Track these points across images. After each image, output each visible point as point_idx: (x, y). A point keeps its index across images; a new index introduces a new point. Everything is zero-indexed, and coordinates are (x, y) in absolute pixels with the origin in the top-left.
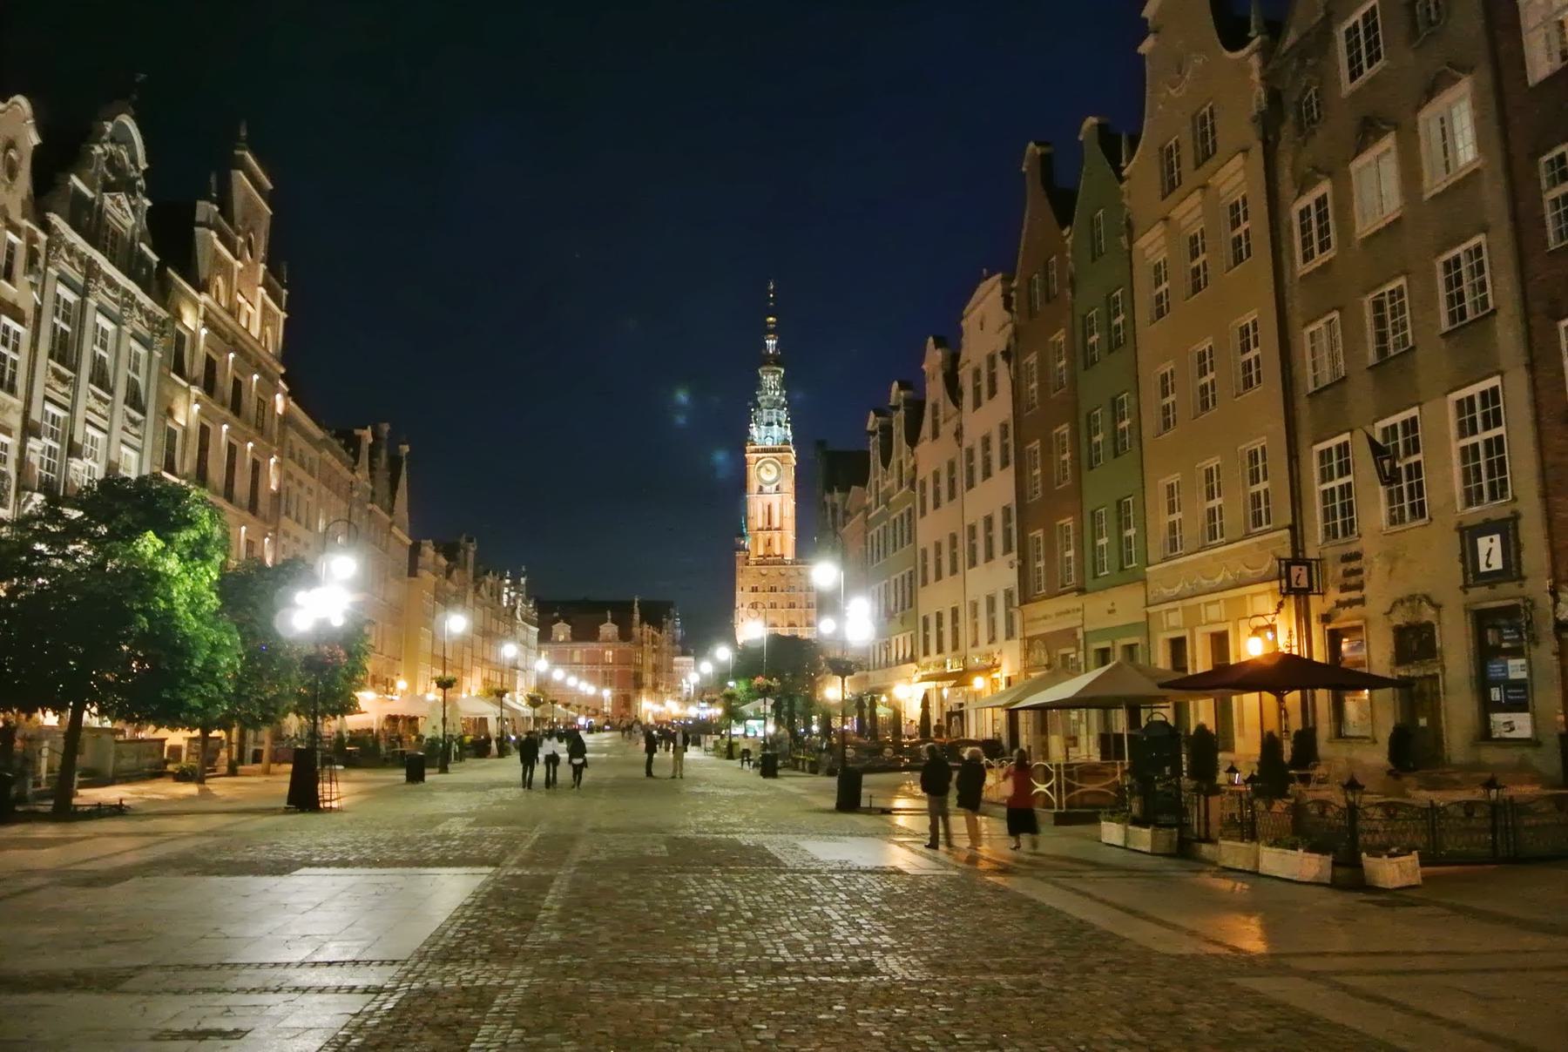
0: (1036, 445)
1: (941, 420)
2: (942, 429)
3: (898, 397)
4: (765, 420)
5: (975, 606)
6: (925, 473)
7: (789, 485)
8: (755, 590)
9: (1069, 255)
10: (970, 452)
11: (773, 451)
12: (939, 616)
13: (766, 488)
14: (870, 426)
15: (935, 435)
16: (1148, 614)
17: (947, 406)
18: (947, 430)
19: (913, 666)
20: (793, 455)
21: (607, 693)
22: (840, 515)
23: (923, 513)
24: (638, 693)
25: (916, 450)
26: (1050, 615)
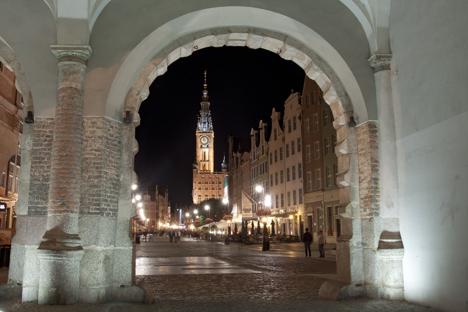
0: (309, 146)
1: (277, 135)
2: (278, 137)
3: (262, 125)
4: (203, 121)
5: (289, 193)
6: (271, 151)
7: (211, 145)
8: (200, 183)
10: (287, 146)
11: (206, 132)
13: (204, 146)
14: (251, 134)
15: (275, 139)
18: (279, 138)
20: (213, 134)
21: (148, 220)
22: (239, 161)
23: (271, 163)
24: (157, 220)
26: (313, 197)
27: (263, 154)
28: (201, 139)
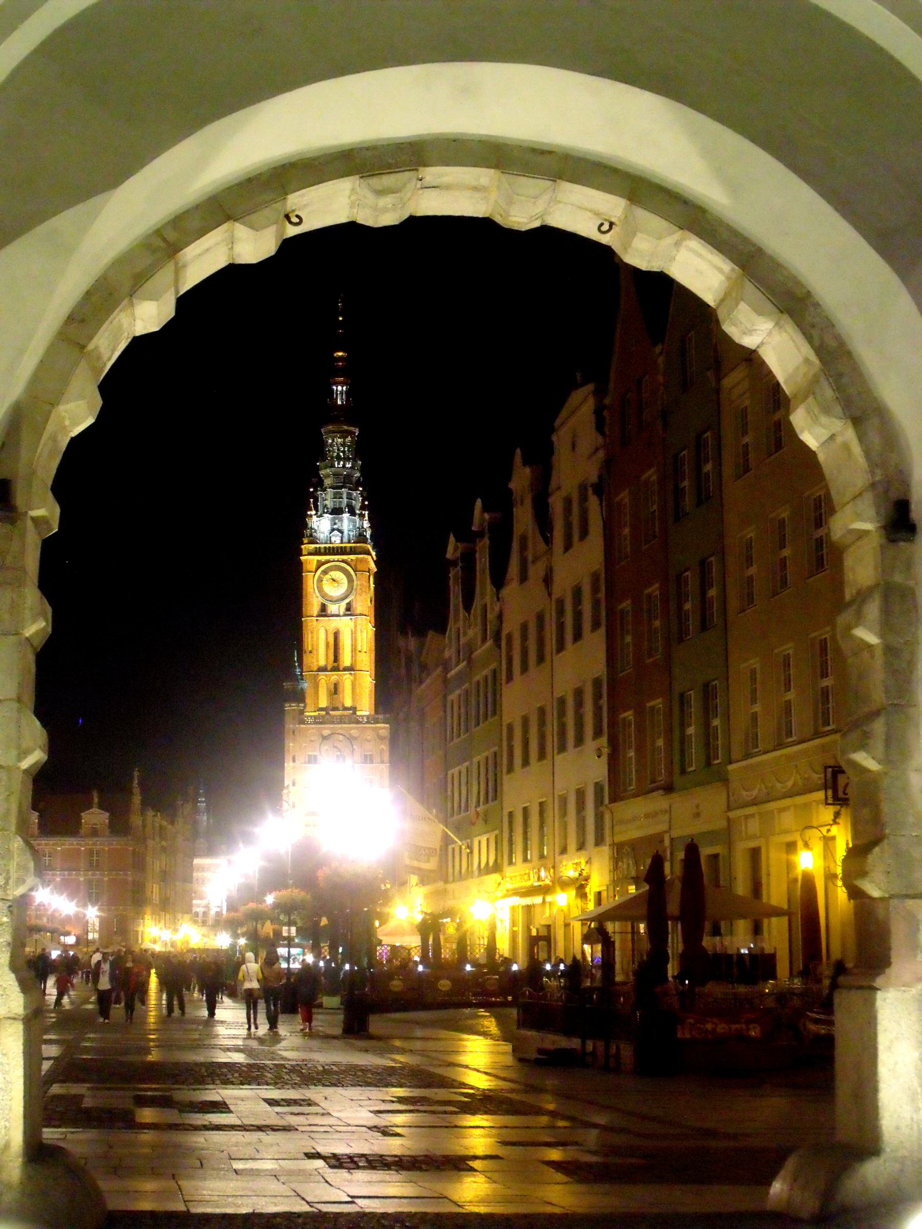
0: (626, 605)
1: (530, 558)
3: (482, 518)
4: (329, 503)
5: (564, 801)
7: (365, 602)
9: (660, 378)
10: (560, 603)
11: (341, 551)
12: (526, 811)
13: (332, 608)
14: (449, 555)
15: (524, 578)
16: (729, 820)
17: (536, 544)
18: (536, 571)
19: (496, 877)
21: (93, 914)
22: (415, 670)
23: (510, 678)
24: (140, 915)
25: (505, 592)
26: (641, 818)
27: (484, 640)
28: (320, 580)
